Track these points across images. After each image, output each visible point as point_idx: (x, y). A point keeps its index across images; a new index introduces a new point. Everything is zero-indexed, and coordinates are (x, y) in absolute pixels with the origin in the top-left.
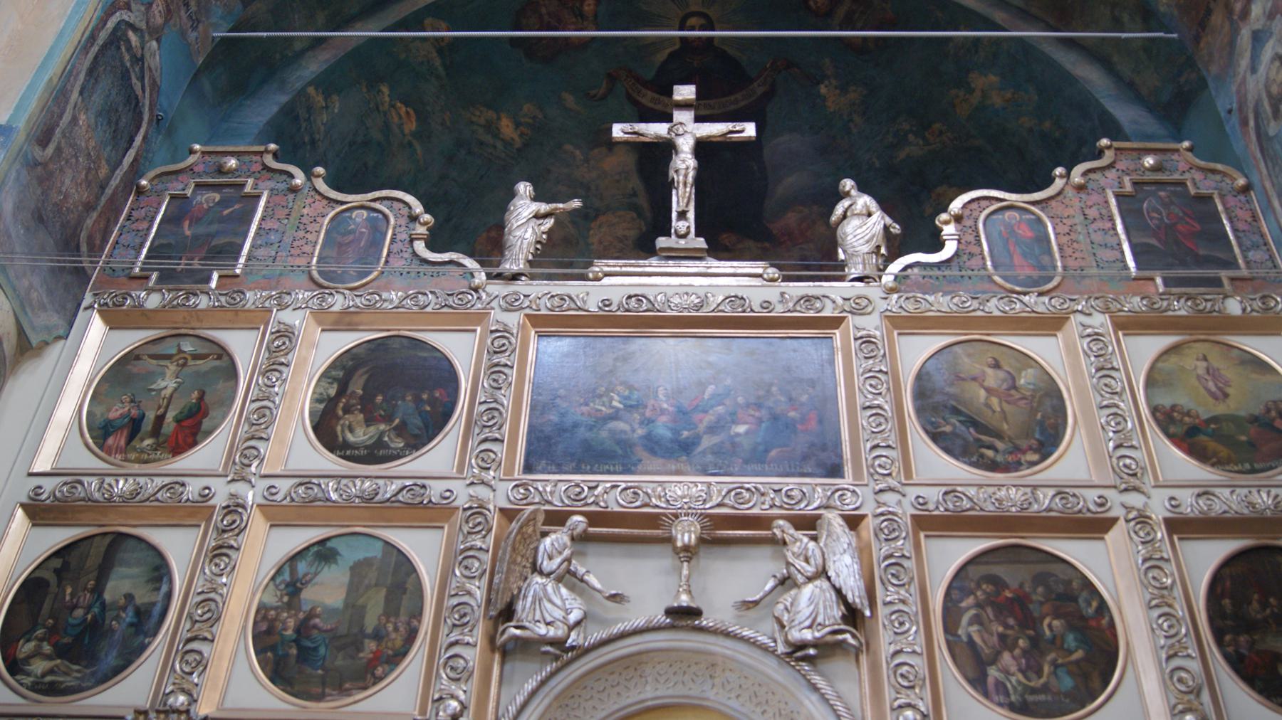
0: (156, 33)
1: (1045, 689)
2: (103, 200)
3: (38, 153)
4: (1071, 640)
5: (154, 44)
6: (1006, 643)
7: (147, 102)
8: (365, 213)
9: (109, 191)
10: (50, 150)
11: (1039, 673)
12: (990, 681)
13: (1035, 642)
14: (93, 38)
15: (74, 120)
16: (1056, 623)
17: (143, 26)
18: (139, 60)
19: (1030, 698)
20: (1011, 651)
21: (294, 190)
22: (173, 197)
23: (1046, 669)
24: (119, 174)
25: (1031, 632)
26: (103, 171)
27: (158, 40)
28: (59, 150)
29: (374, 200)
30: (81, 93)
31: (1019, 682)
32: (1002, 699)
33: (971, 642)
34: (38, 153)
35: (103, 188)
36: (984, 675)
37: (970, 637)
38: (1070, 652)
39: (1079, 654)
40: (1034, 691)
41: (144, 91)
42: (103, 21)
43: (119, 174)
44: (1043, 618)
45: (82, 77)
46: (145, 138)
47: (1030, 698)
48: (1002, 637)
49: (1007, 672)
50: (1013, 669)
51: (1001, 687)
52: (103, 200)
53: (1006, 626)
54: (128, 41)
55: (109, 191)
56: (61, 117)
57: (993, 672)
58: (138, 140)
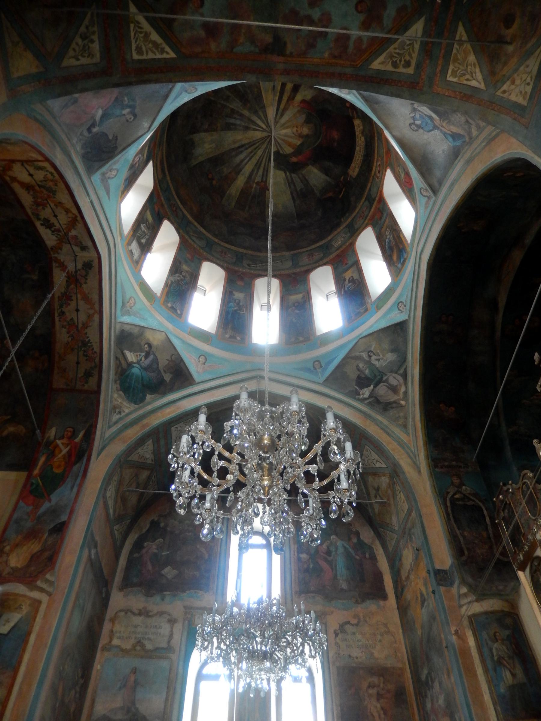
0: (462, 484)
2: (493, 540)
3: (464, 558)
5: (464, 487)
7: (477, 501)
8: (524, 486)
9: (492, 535)
10: (466, 552)
14: (448, 514)
15: (464, 537)
17: (456, 489)
18: (465, 497)
21: (513, 493)
22: (503, 519)
24: (490, 528)
26: (485, 534)
27: (464, 485)
28: (468, 549)
29: (523, 480)
30: (459, 529)
34: (464, 558)
35: (489, 538)
41: (473, 501)
42: (446, 507)
43: (490, 528)
45: (455, 526)
46: (486, 509)
52: (493, 540)
54: (457, 499)
55: (492, 535)
56: (460, 542)
58: (485, 512)
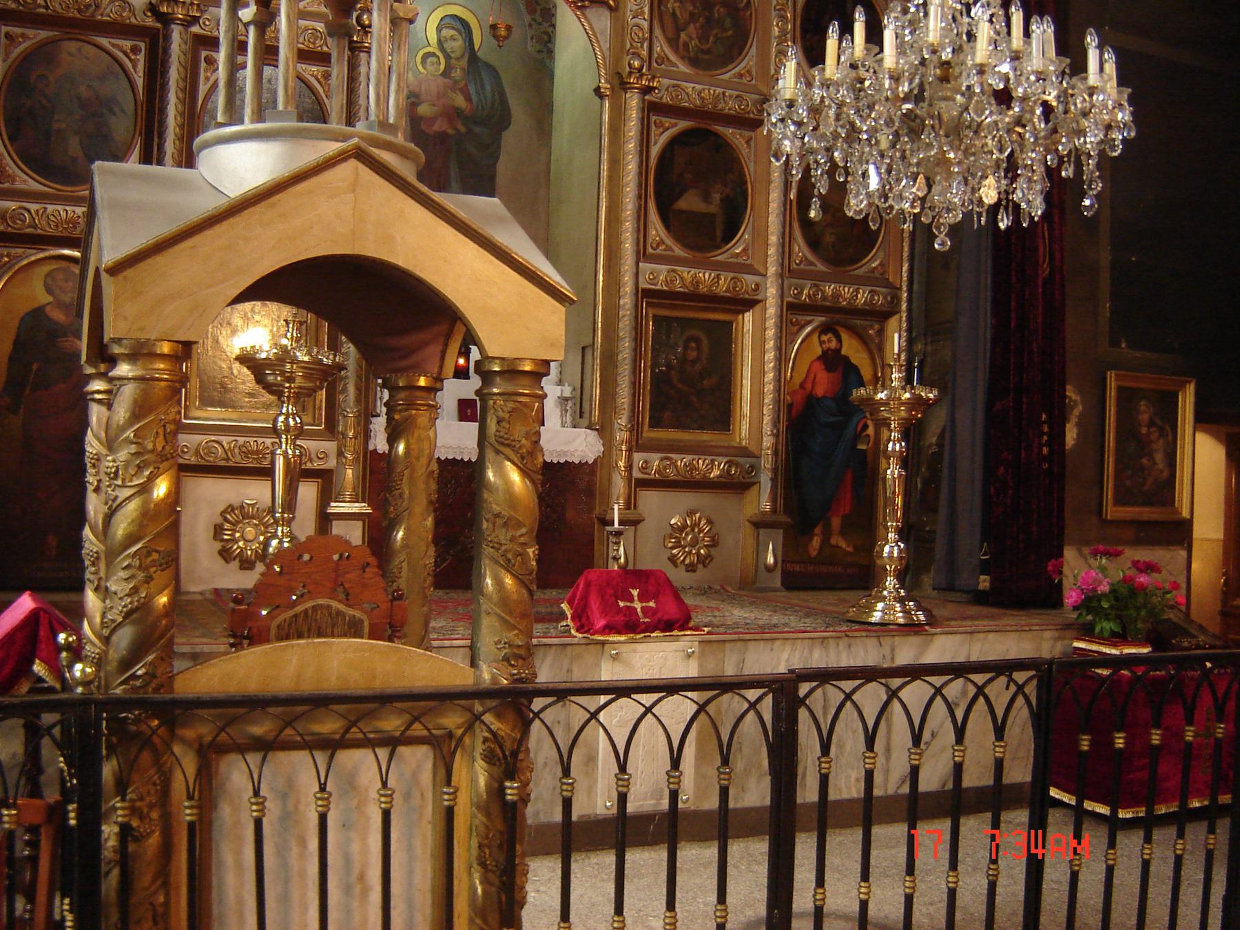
1: (708, 52)
4: (728, 22)
6: (693, 18)
11: (708, 41)
12: (681, 40)
13: (709, 20)
16: (722, 10)
19: (700, 56)
20: (695, 23)
23: (711, 39)
25: (707, 13)
31: (696, 46)
32: (686, 54)
33: (674, 14)
36: (679, 36)
37: (674, 10)
38: (726, 30)
39: (730, 33)
40: (703, 52)
44: (715, 5)
47: (700, 56)
48: (692, 14)
49: (691, 38)
50: (694, 36)
51: (686, 45)
53: (695, 7)
57: (683, 35)
